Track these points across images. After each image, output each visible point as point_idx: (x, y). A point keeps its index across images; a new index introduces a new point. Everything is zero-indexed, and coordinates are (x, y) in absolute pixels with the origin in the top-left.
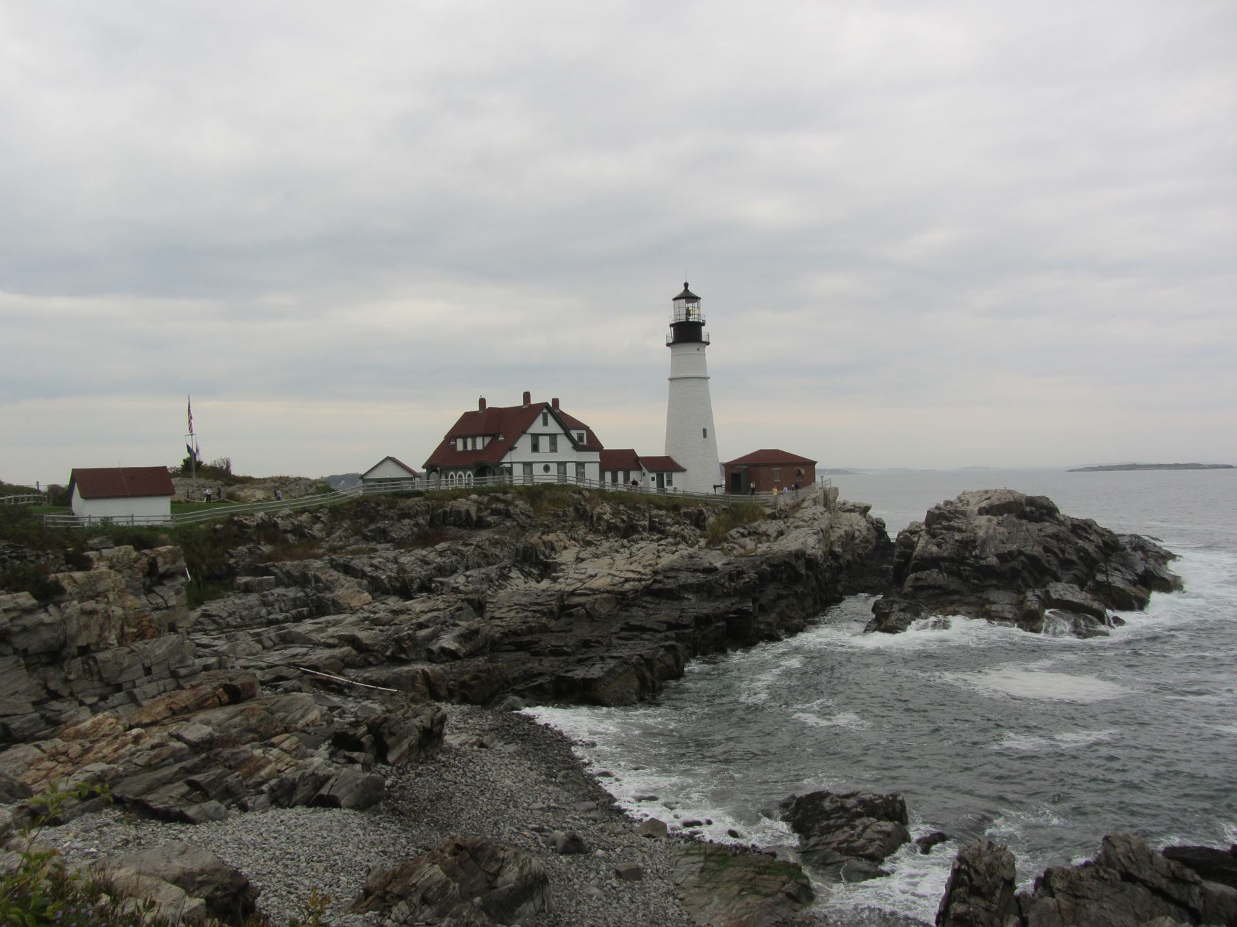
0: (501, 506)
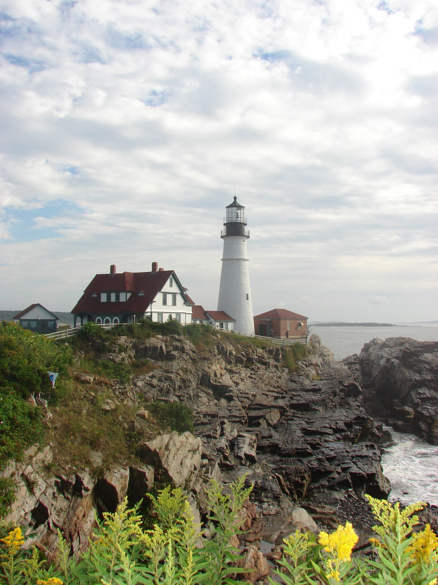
0: (178, 344)
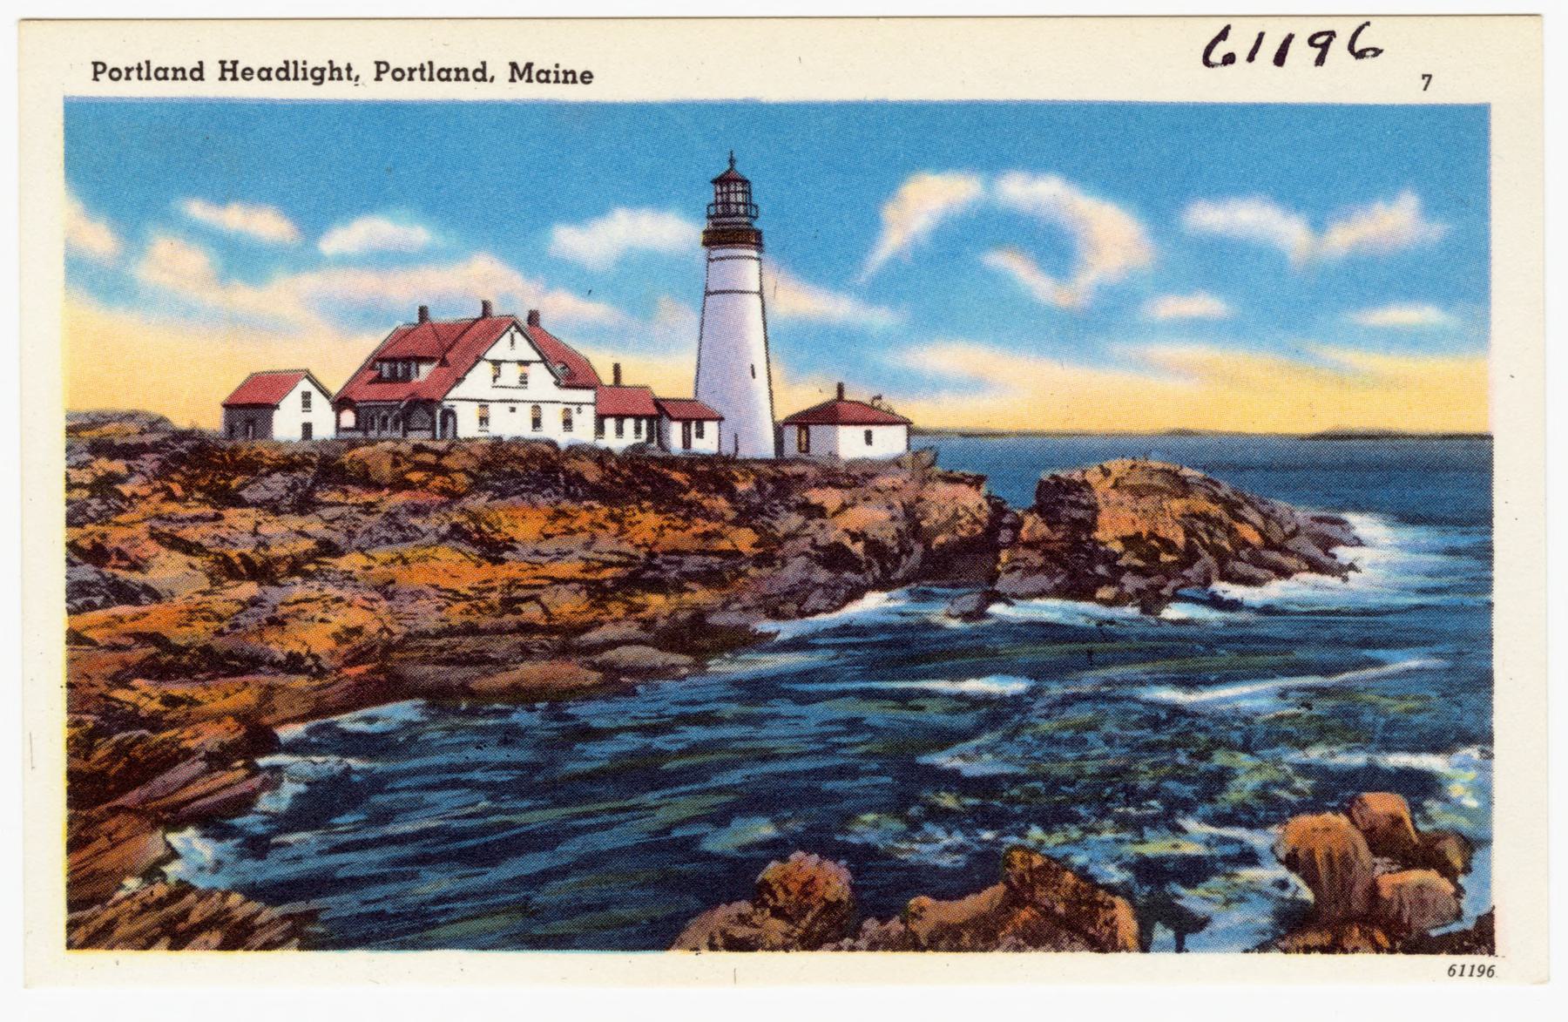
0: (430, 458)
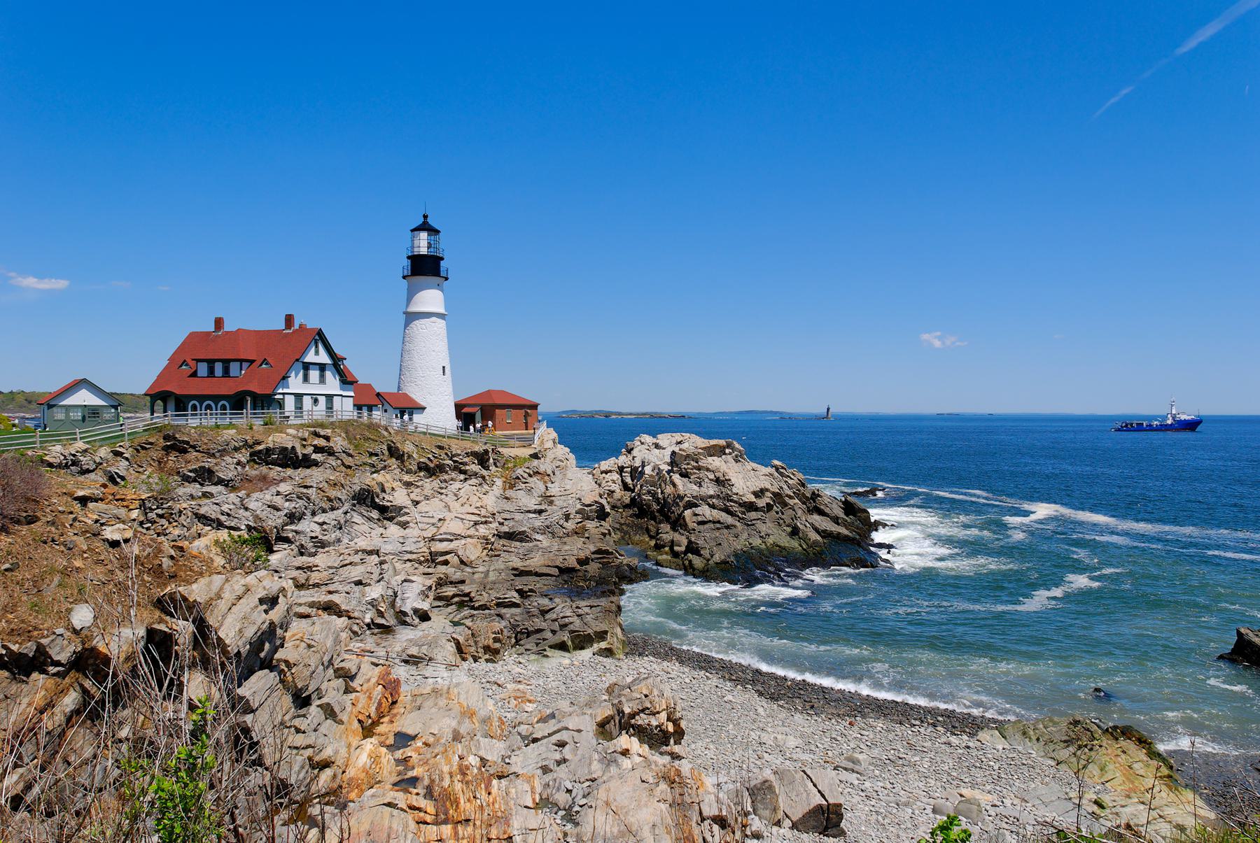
0: (321, 442)
